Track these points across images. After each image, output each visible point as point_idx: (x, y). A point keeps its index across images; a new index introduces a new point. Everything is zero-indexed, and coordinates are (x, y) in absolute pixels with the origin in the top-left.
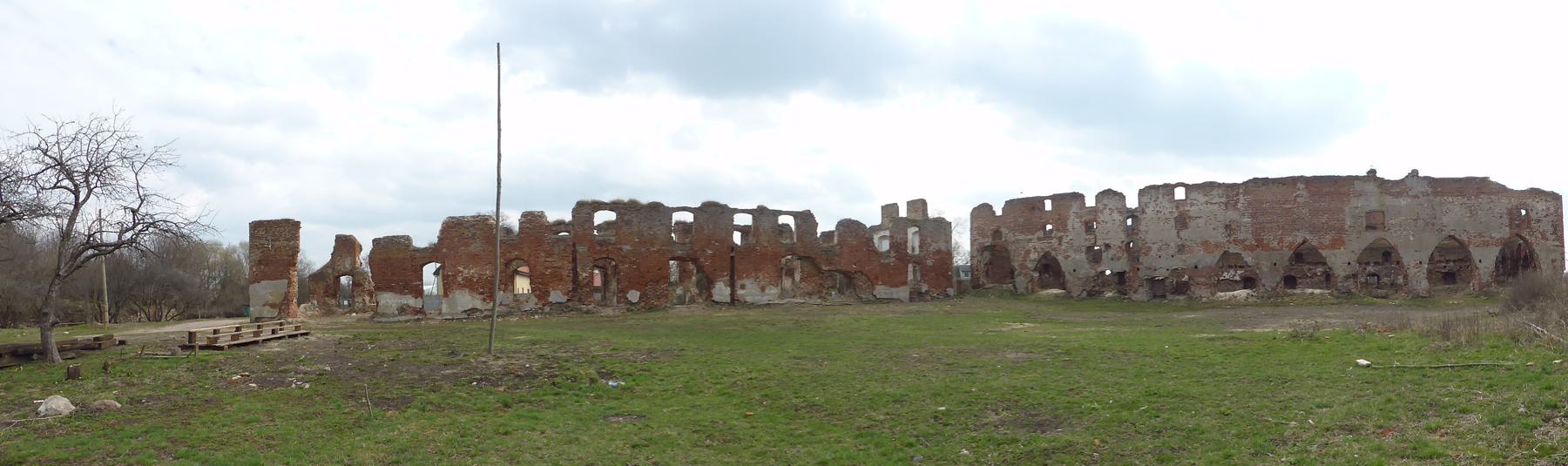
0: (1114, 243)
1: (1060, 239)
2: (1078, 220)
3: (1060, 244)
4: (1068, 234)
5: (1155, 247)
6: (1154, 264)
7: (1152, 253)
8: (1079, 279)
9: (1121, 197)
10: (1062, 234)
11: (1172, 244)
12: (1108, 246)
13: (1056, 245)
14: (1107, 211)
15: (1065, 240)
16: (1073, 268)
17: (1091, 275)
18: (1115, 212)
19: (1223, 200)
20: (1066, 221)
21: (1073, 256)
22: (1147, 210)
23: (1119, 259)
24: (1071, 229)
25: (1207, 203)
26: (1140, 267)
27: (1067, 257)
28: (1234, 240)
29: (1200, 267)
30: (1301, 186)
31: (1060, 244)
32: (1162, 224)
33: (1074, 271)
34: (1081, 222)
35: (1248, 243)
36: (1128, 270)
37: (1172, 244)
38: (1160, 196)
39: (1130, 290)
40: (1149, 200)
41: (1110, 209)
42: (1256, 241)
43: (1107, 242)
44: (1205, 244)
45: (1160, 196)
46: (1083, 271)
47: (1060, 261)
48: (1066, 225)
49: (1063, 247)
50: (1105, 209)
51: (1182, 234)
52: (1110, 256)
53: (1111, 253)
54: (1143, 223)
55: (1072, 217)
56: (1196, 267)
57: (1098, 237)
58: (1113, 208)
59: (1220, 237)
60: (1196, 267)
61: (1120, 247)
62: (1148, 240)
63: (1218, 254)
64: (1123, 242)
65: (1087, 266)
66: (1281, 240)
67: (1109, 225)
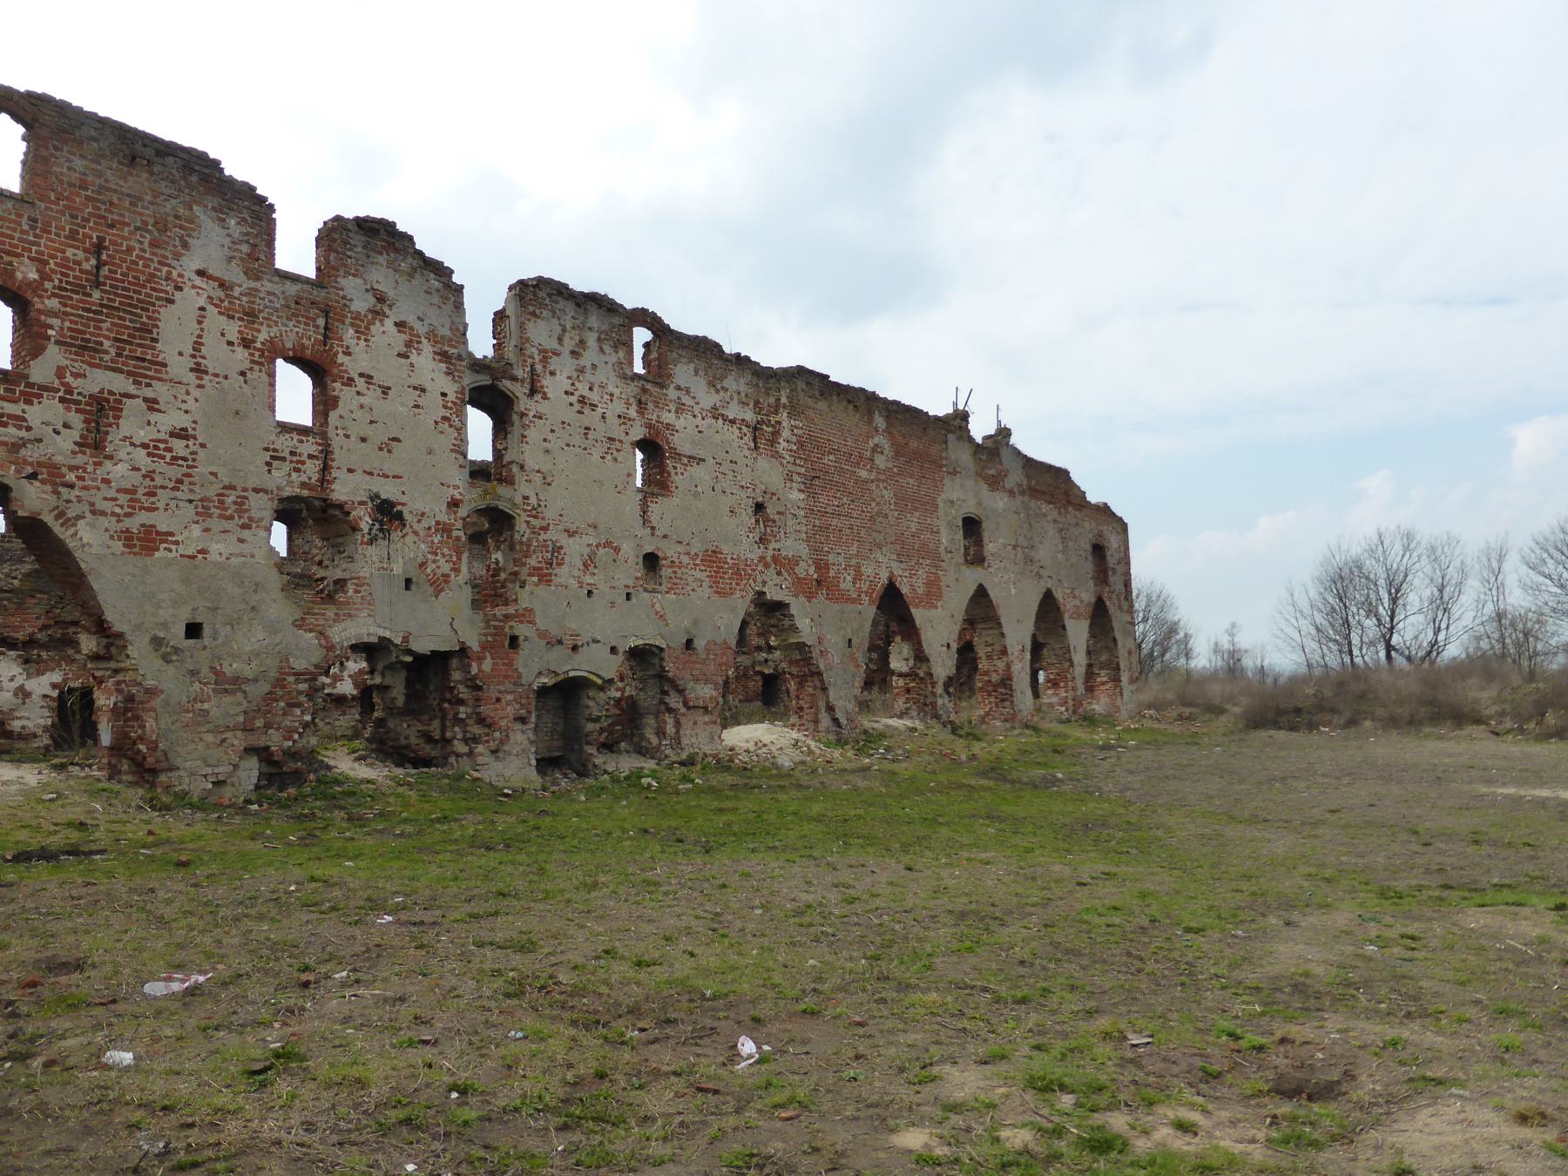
0: (419, 506)
1: (101, 411)
2: (233, 330)
3: (94, 442)
4: (160, 390)
5: (575, 549)
6: (572, 625)
7: (563, 574)
8: (228, 684)
9: (454, 293)
10: (120, 383)
11: (627, 549)
12: (388, 514)
13: (62, 447)
14: (386, 333)
15: (132, 426)
16: (185, 616)
17: (300, 664)
18: (427, 347)
19: (749, 416)
20: (146, 305)
21: (192, 537)
22: (547, 382)
23: (439, 584)
24: (179, 367)
25: (715, 413)
26: (522, 630)
27: (147, 541)
28: (774, 559)
29: (700, 643)
30: (880, 421)
31: (94, 442)
32: (596, 456)
33: (193, 630)
34: (247, 343)
35: (800, 570)
36: (474, 645)
37: (627, 549)
38: (591, 339)
39: (472, 740)
40: (552, 344)
41: (400, 325)
42: (818, 568)
43: (388, 491)
44: (712, 558)
45: (591, 339)
46: (253, 638)
47: (85, 560)
48: (147, 332)
49: (119, 472)
50: (378, 314)
51: (655, 509)
52: (398, 568)
53: (407, 549)
54: (532, 434)
55: (192, 299)
56: (689, 643)
57: (340, 458)
58: (421, 329)
59: (740, 542)
60: (689, 643)
61: (445, 529)
62: (550, 514)
63: (741, 604)
64: (454, 504)
65: (279, 609)
66: (858, 576)
67: (400, 403)
